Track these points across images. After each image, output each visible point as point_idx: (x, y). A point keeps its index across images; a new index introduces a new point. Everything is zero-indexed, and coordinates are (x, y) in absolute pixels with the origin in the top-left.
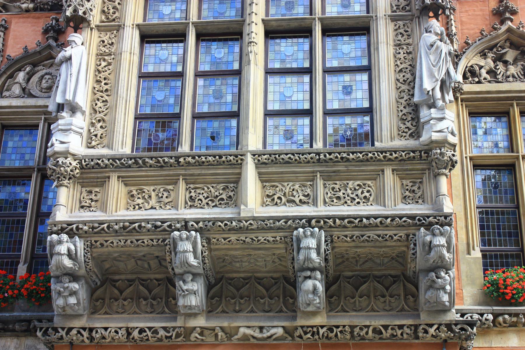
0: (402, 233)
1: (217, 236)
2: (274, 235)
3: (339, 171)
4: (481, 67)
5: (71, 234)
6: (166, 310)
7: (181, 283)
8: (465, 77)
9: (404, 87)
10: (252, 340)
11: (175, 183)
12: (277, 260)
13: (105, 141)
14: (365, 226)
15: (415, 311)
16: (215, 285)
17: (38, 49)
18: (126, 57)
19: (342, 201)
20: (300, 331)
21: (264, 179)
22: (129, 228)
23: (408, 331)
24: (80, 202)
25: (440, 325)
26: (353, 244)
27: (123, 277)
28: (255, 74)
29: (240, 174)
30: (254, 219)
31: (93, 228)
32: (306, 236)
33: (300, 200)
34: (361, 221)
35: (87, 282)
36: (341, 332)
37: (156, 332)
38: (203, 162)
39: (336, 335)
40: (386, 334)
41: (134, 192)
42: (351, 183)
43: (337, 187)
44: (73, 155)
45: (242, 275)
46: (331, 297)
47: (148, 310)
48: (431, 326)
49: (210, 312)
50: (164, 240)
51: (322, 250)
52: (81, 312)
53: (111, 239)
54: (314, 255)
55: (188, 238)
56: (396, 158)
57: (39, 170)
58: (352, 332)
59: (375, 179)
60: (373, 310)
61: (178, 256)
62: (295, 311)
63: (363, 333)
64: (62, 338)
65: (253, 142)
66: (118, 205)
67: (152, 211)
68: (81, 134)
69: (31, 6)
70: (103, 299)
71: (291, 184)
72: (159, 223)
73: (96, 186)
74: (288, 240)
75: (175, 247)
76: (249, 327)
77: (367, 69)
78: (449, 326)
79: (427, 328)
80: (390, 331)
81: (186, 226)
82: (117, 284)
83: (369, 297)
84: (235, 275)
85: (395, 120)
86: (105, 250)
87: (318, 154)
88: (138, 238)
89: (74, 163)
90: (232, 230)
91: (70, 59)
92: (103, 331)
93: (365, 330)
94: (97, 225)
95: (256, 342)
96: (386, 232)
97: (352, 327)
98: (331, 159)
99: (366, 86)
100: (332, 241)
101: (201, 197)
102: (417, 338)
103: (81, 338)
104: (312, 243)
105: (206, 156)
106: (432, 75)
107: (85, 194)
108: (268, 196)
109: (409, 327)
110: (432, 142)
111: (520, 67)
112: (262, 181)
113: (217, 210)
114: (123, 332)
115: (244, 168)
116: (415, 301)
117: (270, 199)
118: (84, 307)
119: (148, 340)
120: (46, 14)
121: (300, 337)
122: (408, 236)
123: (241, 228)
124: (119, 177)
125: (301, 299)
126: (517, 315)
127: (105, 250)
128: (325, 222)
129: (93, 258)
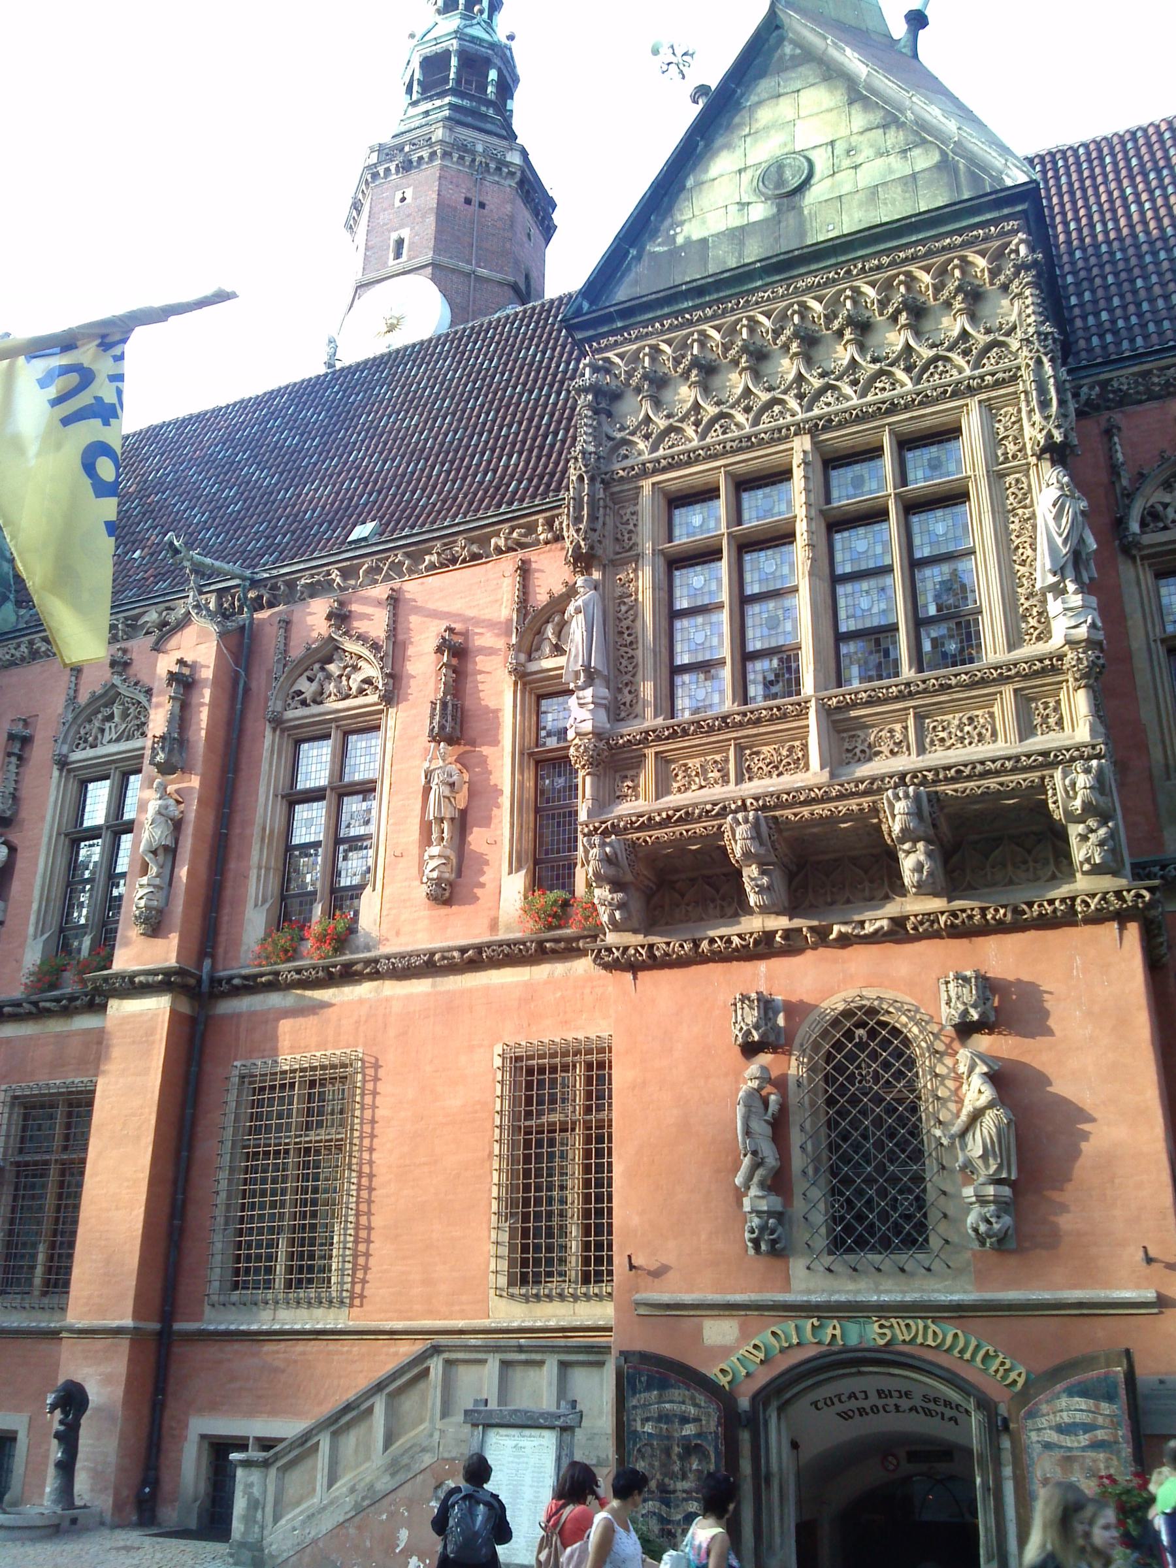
4: (1166, 506)
8: (1143, 524)
31: (632, 823)
46: (953, 871)
49: (795, 908)
51: (926, 813)
68: (605, 706)
69: (550, 536)
70: (662, 907)
71: (876, 730)
72: (709, 807)
93: (1002, 911)
108: (848, 751)
109: (1063, 900)
112: (839, 732)
122: (1043, 778)
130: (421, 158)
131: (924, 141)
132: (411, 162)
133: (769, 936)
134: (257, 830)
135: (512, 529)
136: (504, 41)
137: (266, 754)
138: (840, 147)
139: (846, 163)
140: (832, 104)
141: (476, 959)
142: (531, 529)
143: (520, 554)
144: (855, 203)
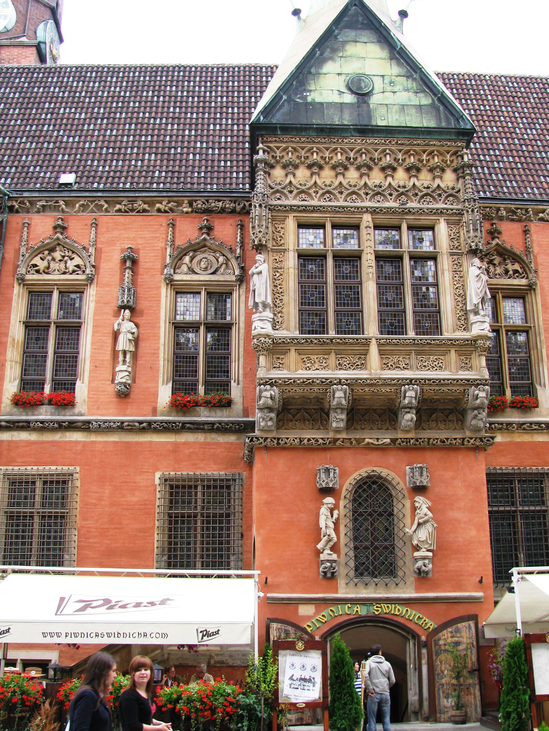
0: (462, 389)
5: (272, 385)
9: (459, 299)
21: (381, 353)
37: (317, 441)
53: (295, 388)
58: (428, 442)
67: (317, 372)
69: (190, 210)
81: (340, 383)
86: (291, 394)
90: (369, 385)
97: (429, 439)
102: (463, 444)
107: (275, 360)
113: (355, 372)
117: (385, 366)
125: (403, 423)
131: (423, 91)
133: (336, 440)
134: (10, 340)
137: (15, 297)
138: (387, 80)
139: (389, 88)
141: (148, 427)
142: (179, 204)
144: (394, 110)
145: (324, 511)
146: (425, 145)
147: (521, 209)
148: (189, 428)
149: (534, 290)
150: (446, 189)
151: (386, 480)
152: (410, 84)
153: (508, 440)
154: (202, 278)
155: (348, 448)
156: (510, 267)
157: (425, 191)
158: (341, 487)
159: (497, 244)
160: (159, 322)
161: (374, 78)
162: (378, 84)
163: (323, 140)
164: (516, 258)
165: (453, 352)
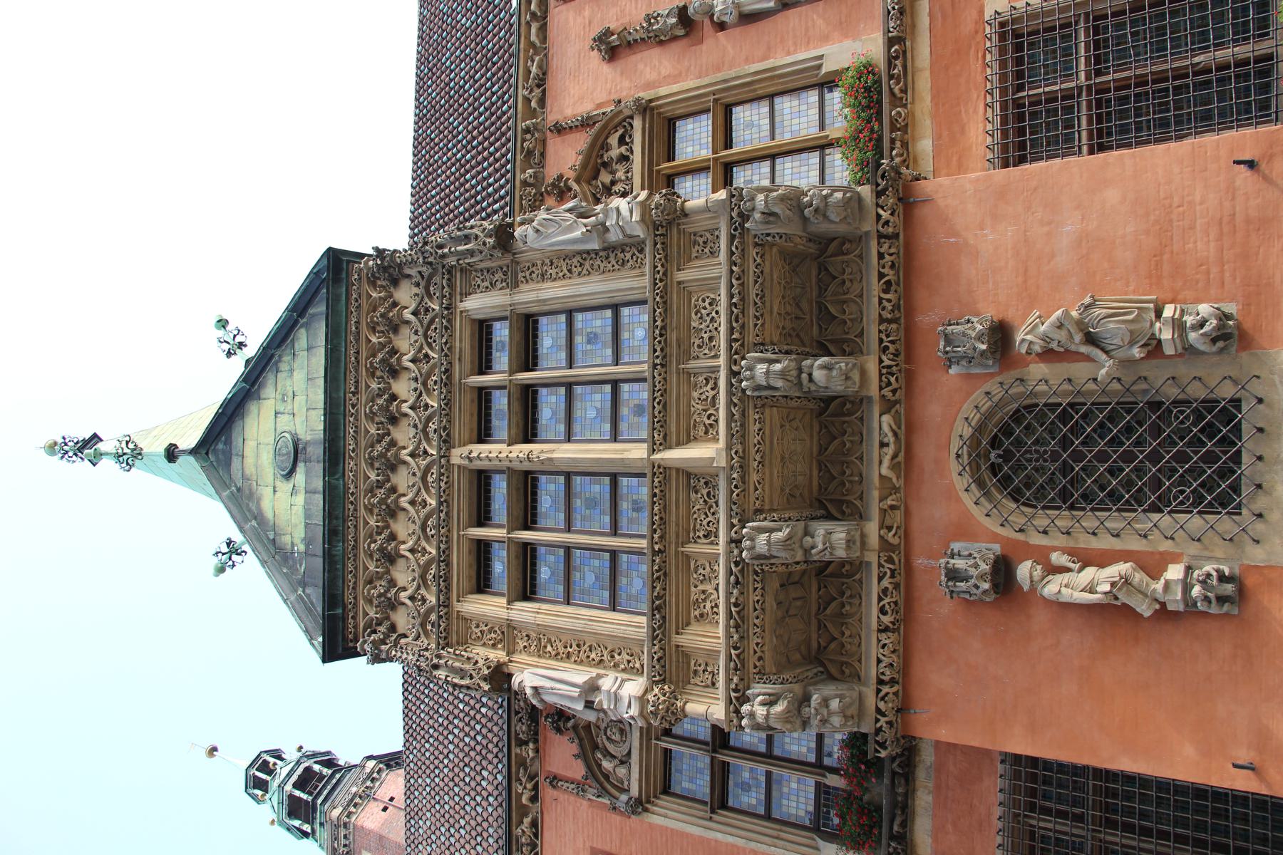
0: (753, 252)
1: (752, 499)
2: (752, 421)
3: (678, 340)
5: (744, 699)
6: (857, 577)
7: (813, 551)
9: (587, 265)
10: (899, 459)
11: (688, 557)
12: (794, 424)
13: (636, 650)
14: (743, 299)
15: (861, 239)
16: (826, 509)
17: (576, 741)
18: (541, 619)
19: (715, 333)
20: (887, 392)
21: (687, 439)
22: (738, 621)
23: (886, 246)
24: (707, 686)
25: (878, 205)
26: (767, 316)
27: (814, 636)
28: (565, 452)
29: (678, 470)
30: (729, 447)
31: (736, 669)
32: (752, 378)
33: (712, 389)
34: (735, 305)
35: (815, 684)
36: (888, 336)
38: (661, 518)
39: (892, 342)
40: (890, 275)
41: (697, 613)
42: (694, 324)
43: (697, 342)
44: (646, 692)
45: (815, 473)
47: (857, 601)
48: (879, 216)
49: (861, 517)
50: (756, 573)
51: (774, 356)
52: (855, 695)
54: (778, 367)
55: (752, 540)
56: (662, 265)
57: (714, 751)
59: (690, 293)
60: (861, 296)
61: (775, 553)
62: (861, 400)
63: (889, 306)
64: (890, 723)
65: (638, 452)
66: (709, 637)
68: (623, 681)
70: (842, 663)
73: (689, 664)
74: (759, 403)
75: (765, 557)
76: (880, 462)
77: (570, 313)
78: (879, 194)
79: (881, 222)
80: (886, 271)
82: (823, 644)
83: (844, 302)
84: (815, 483)
85: (624, 273)
87: (655, 365)
88: (751, 609)
89: (656, 690)
90: (743, 479)
91: (535, 689)
92: (882, 665)
94: (732, 664)
95: (902, 454)
96: (751, 273)
97: (882, 320)
98: (662, 350)
99: (589, 315)
100: (763, 344)
101: (705, 523)
102: (896, 236)
103: (891, 695)
104: (761, 368)
105: (653, 515)
106: (570, 229)
108: (706, 433)
110: (643, 220)
111: (618, 167)
112: (689, 441)
114: (883, 636)
115: (669, 464)
116: (850, 241)
118: (848, 689)
119: (896, 603)
120: (541, 729)
121: (894, 391)
122: (756, 245)
123: (741, 467)
124: (678, 633)
125: (838, 387)
126: (893, 141)
127: (767, 656)
128: (736, 353)
129: (778, 672)
130: (345, 837)
131: (293, 341)
132: (345, 846)
135: (519, 780)
136: (300, 754)
140: (256, 411)
142: (522, 763)
143: (540, 779)
145: (1052, 587)
146: (357, 340)
147: (524, 140)
148: (904, 824)
149: (651, 101)
150: (418, 299)
151: (980, 429)
152: (284, 366)
153: (928, 122)
154: (636, 743)
155: (907, 513)
156: (615, 152)
157: (422, 340)
158: (995, 538)
159: (578, 181)
160: (709, 840)
161: (279, 431)
162: (285, 423)
163: (352, 529)
164: (599, 145)
165: (681, 276)
